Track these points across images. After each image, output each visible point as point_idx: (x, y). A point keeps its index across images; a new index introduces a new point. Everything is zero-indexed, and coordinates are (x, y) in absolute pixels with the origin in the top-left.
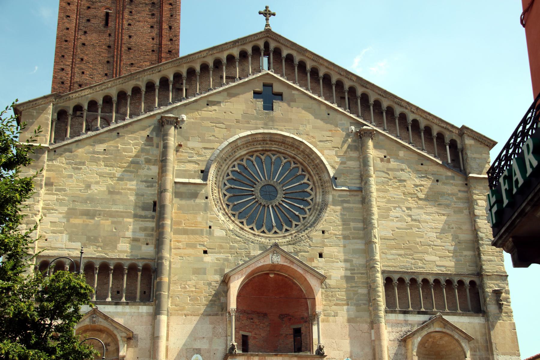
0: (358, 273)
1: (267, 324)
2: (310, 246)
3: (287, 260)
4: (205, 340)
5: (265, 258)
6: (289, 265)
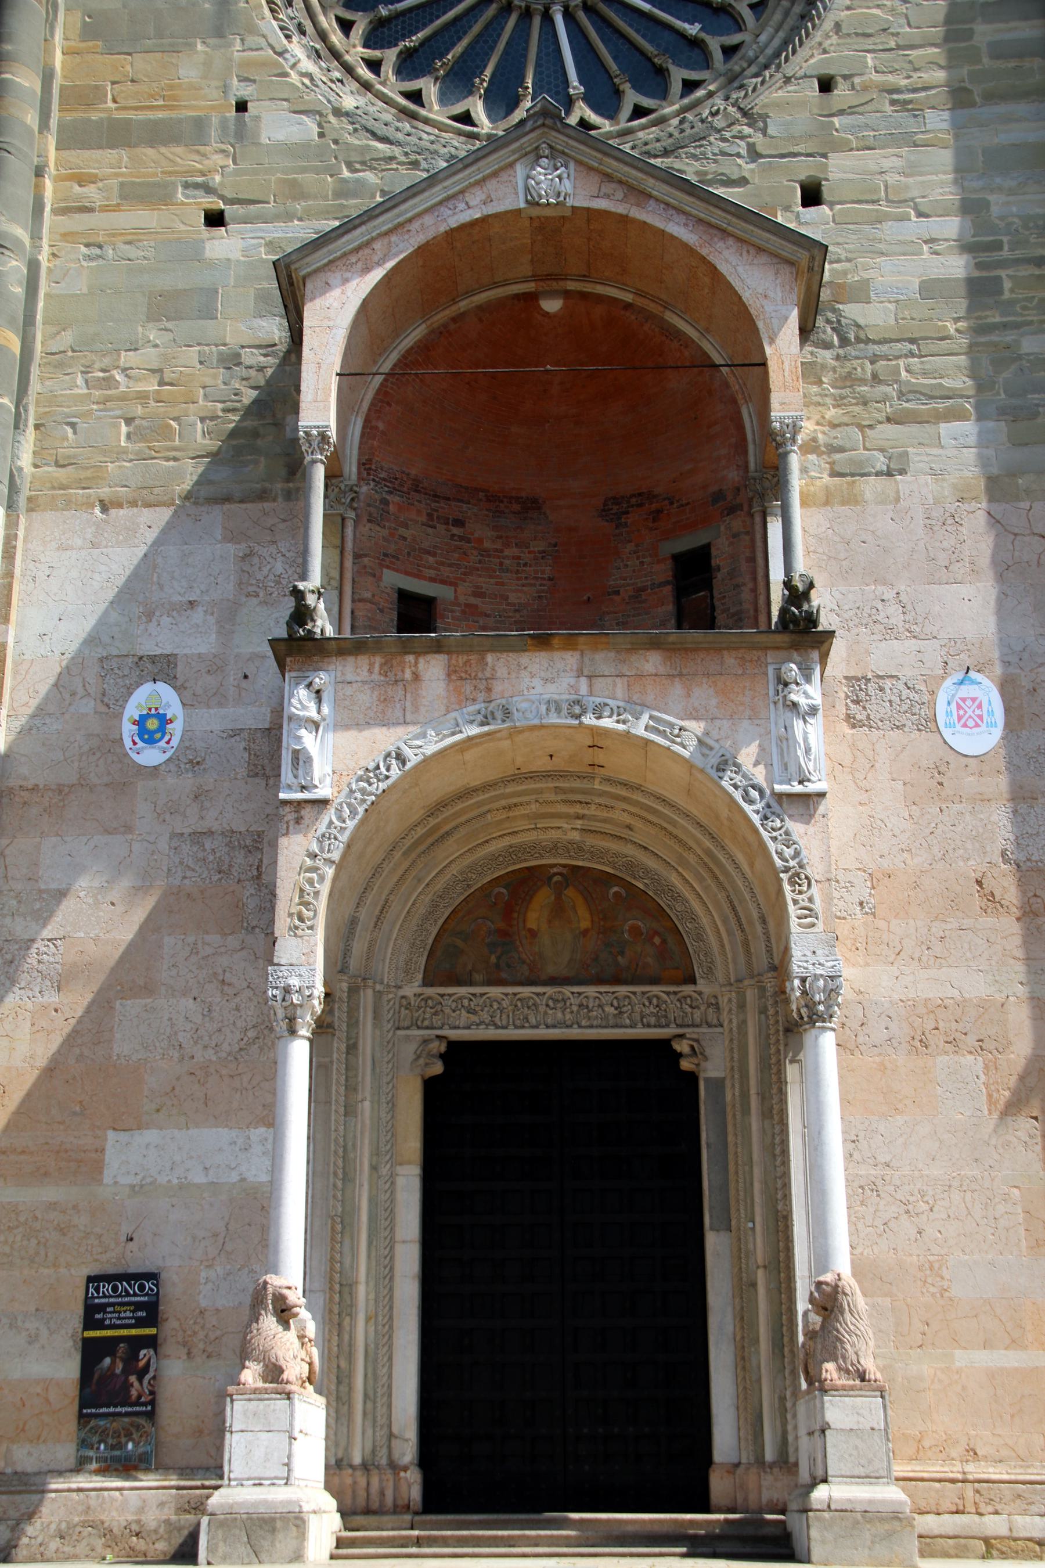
1: (539, 546)
2: (754, 154)
3: (608, 188)
4: (198, 616)
5: (492, 185)
6: (620, 209)
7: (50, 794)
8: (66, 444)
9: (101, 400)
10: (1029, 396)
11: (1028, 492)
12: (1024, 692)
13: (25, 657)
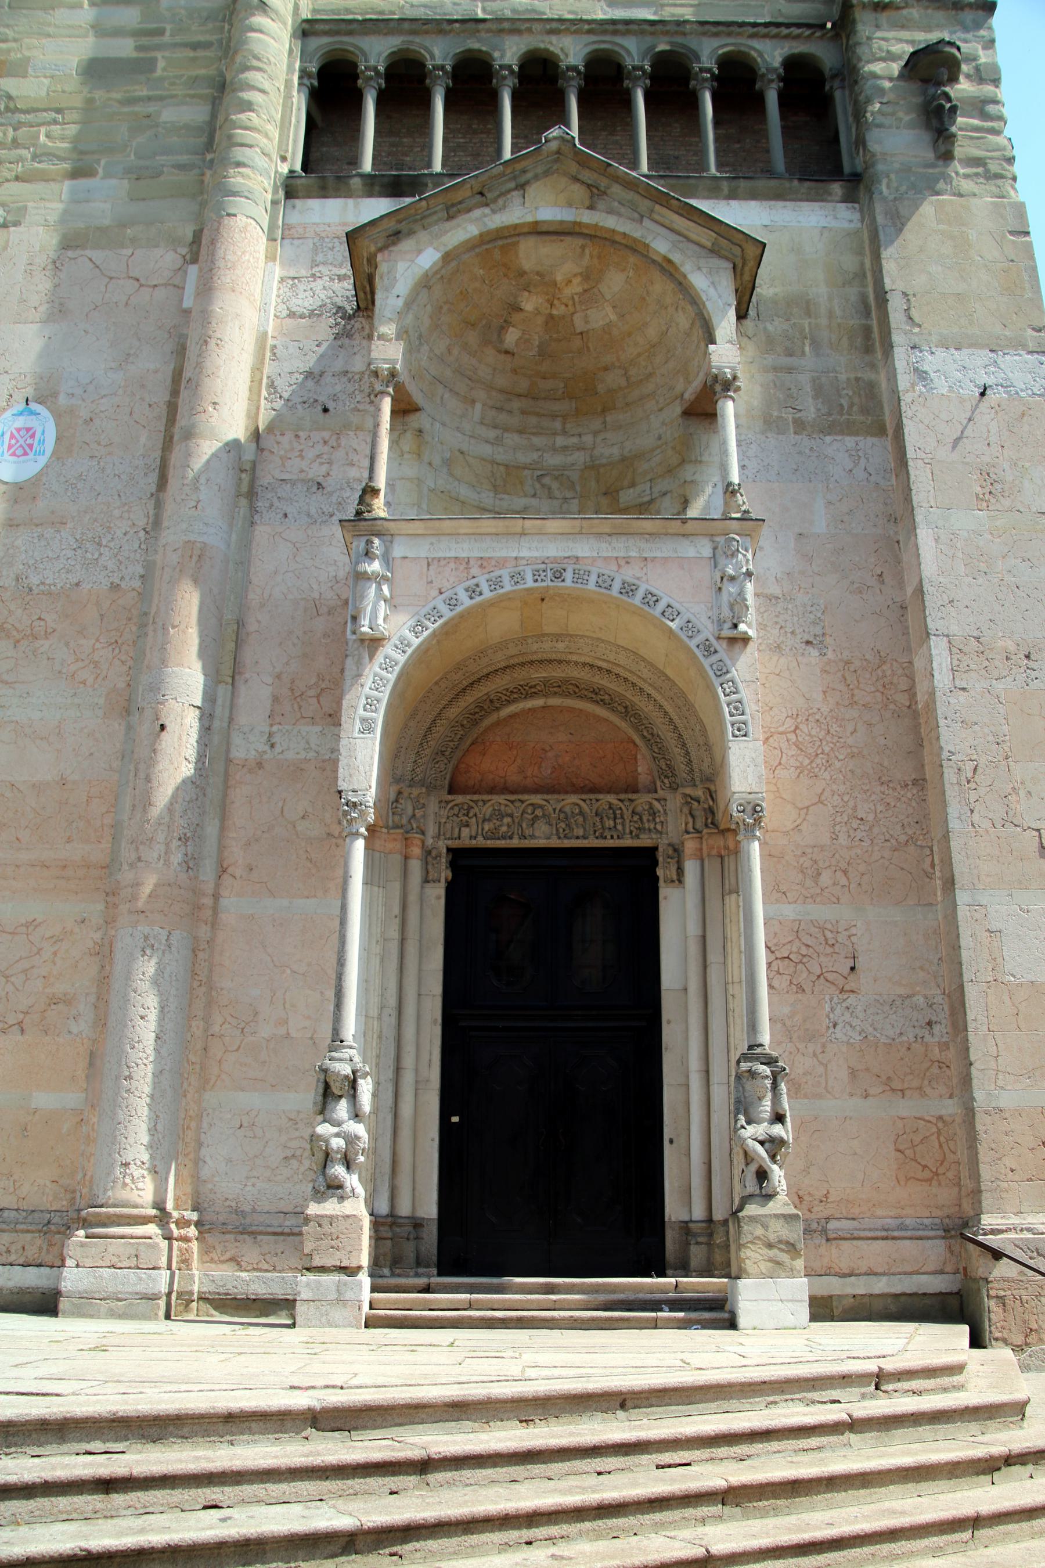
0: (175, 45)
10: (158, 158)
11: (133, 240)
12: (80, 422)
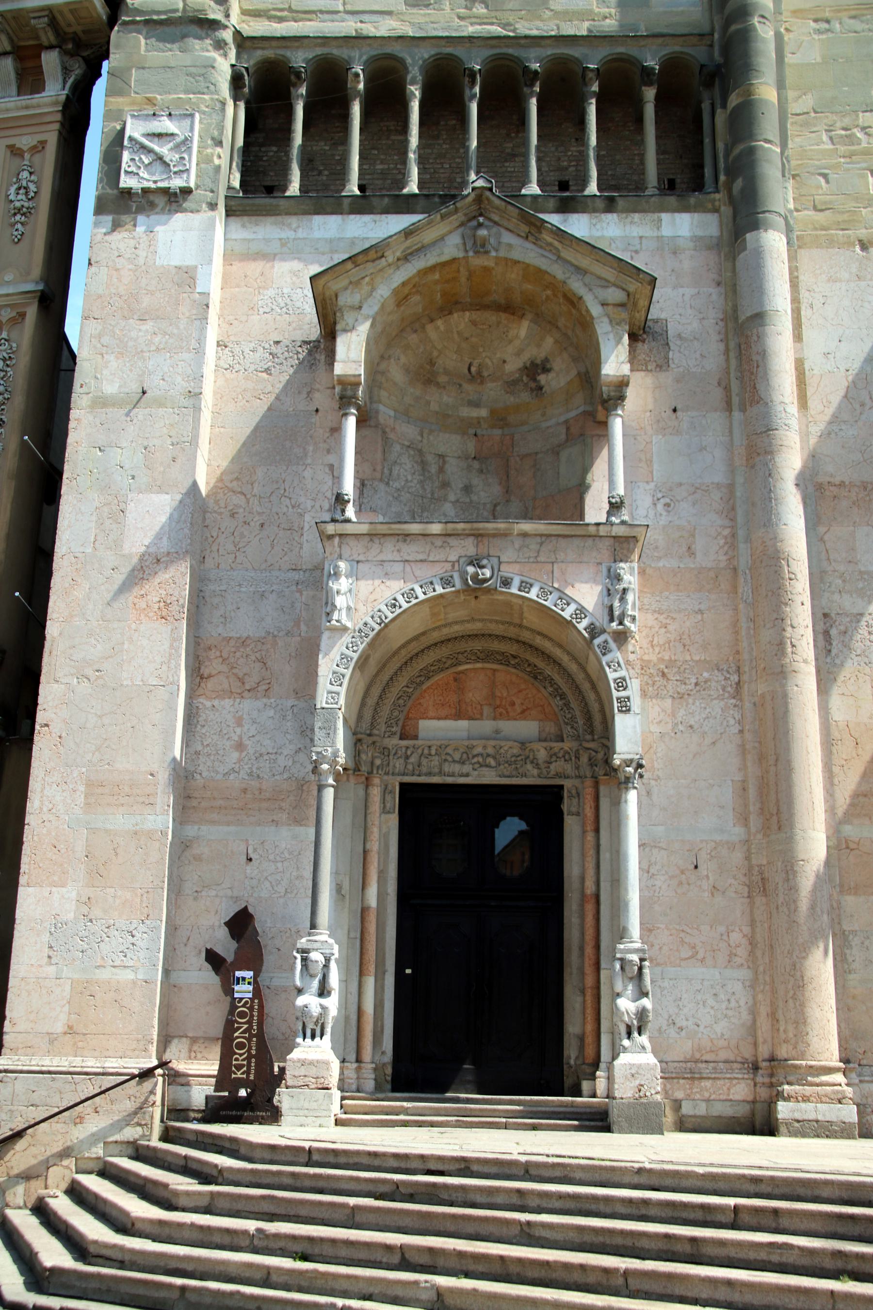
7: (856, 489)
8: (820, 192)
9: (847, 154)
13: (815, 372)
